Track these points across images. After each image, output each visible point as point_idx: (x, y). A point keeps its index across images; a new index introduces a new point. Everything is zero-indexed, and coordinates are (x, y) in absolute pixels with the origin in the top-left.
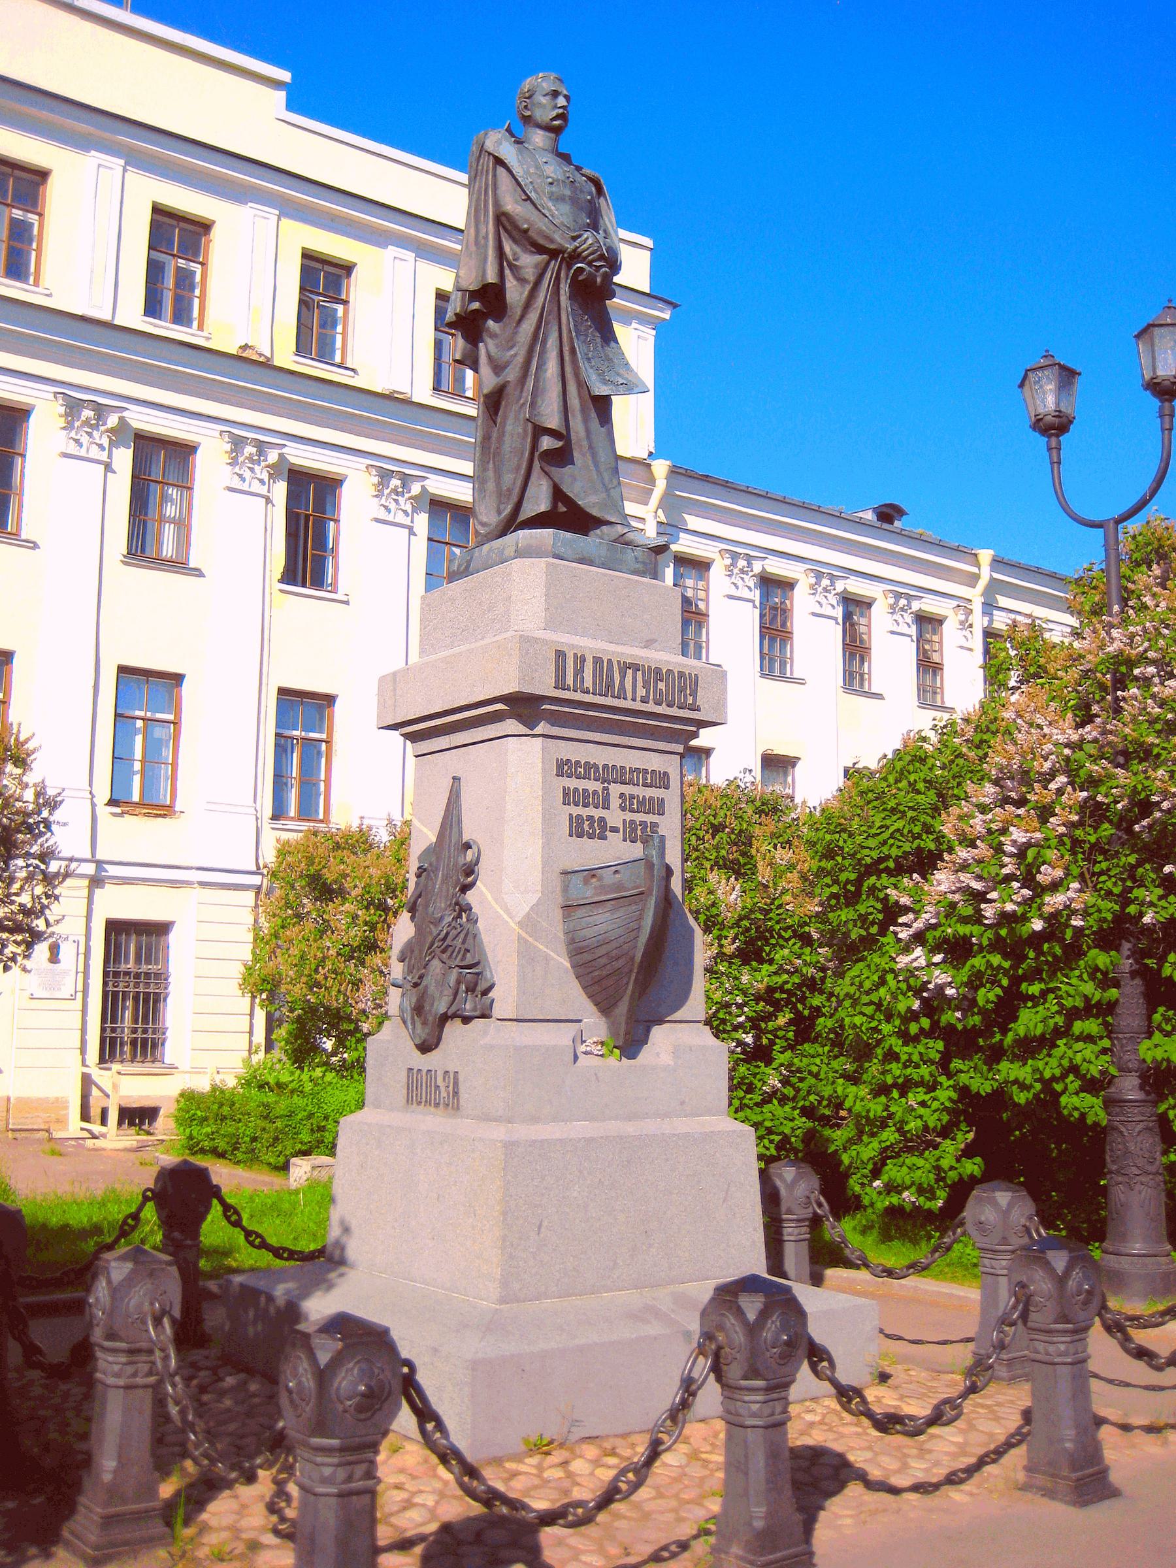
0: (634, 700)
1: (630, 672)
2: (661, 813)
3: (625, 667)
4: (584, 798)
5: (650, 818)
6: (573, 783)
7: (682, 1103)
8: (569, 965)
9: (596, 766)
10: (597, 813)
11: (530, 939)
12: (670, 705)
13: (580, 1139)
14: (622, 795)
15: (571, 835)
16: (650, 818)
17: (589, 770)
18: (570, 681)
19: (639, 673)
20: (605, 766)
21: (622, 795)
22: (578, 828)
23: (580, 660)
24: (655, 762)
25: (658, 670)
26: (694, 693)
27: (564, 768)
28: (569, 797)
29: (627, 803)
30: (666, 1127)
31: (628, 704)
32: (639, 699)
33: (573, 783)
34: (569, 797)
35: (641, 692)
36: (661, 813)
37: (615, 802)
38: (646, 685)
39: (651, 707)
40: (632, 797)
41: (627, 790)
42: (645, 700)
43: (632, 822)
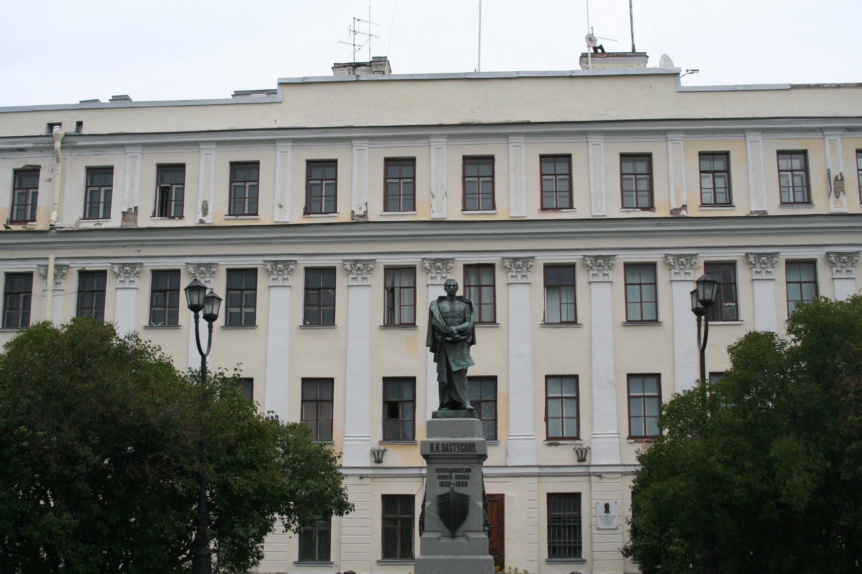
3: (451, 444)
4: (445, 477)
6: (441, 474)
10: (448, 481)
17: (446, 470)
22: (442, 485)
24: (466, 467)
25: (462, 444)
27: (438, 470)
28: (439, 477)
30: (460, 557)
33: (441, 474)
34: (439, 477)
37: (454, 477)
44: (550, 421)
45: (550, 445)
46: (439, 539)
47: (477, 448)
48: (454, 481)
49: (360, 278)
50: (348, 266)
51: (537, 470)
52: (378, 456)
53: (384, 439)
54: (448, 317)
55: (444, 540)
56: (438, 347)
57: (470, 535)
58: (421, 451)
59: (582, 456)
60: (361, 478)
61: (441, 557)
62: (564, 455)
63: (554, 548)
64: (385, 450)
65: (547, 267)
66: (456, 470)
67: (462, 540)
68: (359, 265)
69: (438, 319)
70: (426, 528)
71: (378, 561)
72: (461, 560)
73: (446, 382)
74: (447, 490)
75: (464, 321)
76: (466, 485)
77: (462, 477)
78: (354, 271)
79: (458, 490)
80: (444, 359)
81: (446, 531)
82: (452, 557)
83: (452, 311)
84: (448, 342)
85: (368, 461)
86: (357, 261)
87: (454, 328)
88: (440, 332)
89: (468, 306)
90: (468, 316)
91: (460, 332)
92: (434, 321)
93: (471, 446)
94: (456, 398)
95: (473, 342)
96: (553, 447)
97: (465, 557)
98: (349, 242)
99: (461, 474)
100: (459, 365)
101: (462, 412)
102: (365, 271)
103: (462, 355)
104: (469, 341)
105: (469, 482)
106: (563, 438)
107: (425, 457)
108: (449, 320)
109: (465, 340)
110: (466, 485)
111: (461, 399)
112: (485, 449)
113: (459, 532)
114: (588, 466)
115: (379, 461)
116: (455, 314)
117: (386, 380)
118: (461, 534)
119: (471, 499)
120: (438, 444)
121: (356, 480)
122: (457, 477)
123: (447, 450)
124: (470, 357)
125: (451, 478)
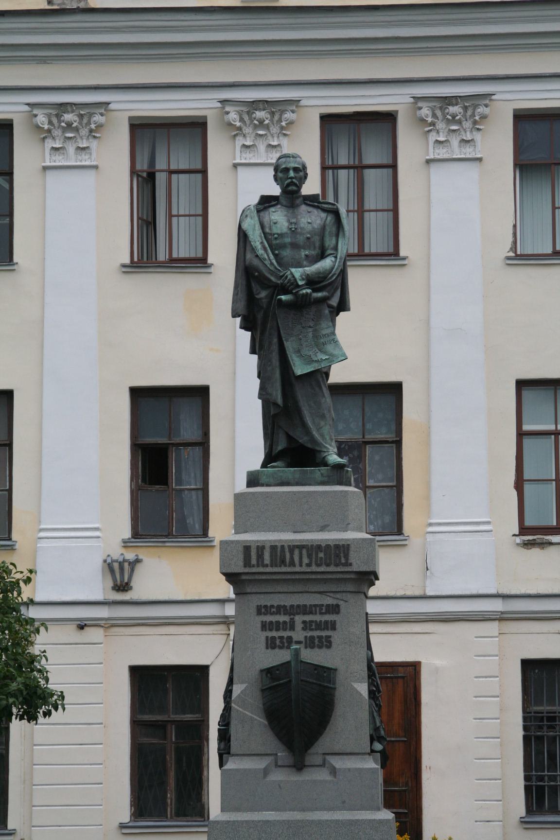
0: (301, 565)
1: (297, 552)
2: (334, 628)
3: (292, 548)
4: (277, 626)
5: (324, 633)
6: (269, 618)
7: (344, 802)
8: (266, 723)
9: (285, 606)
10: (285, 634)
12: (328, 565)
13: (259, 821)
14: (304, 622)
15: (267, 648)
16: (324, 633)
17: (280, 609)
18: (254, 561)
19: (304, 552)
20: (292, 606)
21: (304, 622)
24: (328, 601)
25: (319, 547)
26: (347, 556)
27: (261, 610)
28: (264, 626)
31: (297, 569)
32: (304, 564)
33: (269, 618)
34: (264, 626)
35: (306, 560)
36: (334, 628)
37: (299, 626)
38: (309, 556)
39: (314, 568)
40: (311, 622)
41: (308, 618)
42: (309, 565)
43: (312, 638)
44: (527, 487)
45: (527, 545)
46: (266, 772)
47: (353, 557)
48: (299, 634)
49: (71, 149)
50: (42, 119)
51: (497, 606)
52: (120, 575)
53: (136, 534)
54: (283, 246)
55: (278, 776)
56: (260, 316)
57: (338, 763)
58: (222, 565)
60: (81, 627)
61: (270, 816)
63: (540, 790)
64: (138, 561)
65: (522, 118)
66: (304, 610)
67: (322, 775)
68: (68, 117)
69: (261, 252)
70: (234, 747)
71: (122, 826)
72: (320, 823)
73: (280, 401)
74: (282, 656)
75: (322, 256)
76: (329, 645)
77: (319, 626)
78: (57, 133)
79: (311, 656)
80: (275, 347)
81: (283, 754)
82: (297, 816)
83: (294, 232)
84: (284, 305)
85: (96, 588)
86: (63, 107)
87: (297, 272)
88: (264, 282)
89: (330, 218)
90: (330, 242)
91: (313, 282)
92: (249, 256)
93: (339, 552)
94: (303, 440)
95: (343, 306)
96: (535, 551)
97: (326, 816)
98: (44, 60)
99: (317, 618)
100: (310, 361)
101: (318, 472)
102: (84, 132)
103: (316, 337)
104: (334, 302)
105: (336, 637)
107: (231, 577)
108: (287, 253)
109: (324, 300)
110: (329, 645)
111: (313, 440)
112: (372, 558)
113: (313, 756)
115: (123, 587)
116: (301, 239)
117: (137, 393)
118: (318, 760)
119: (340, 677)
120: (261, 549)
121: (69, 633)
122: (307, 626)
123: (283, 562)
124: (335, 342)
125: (292, 628)
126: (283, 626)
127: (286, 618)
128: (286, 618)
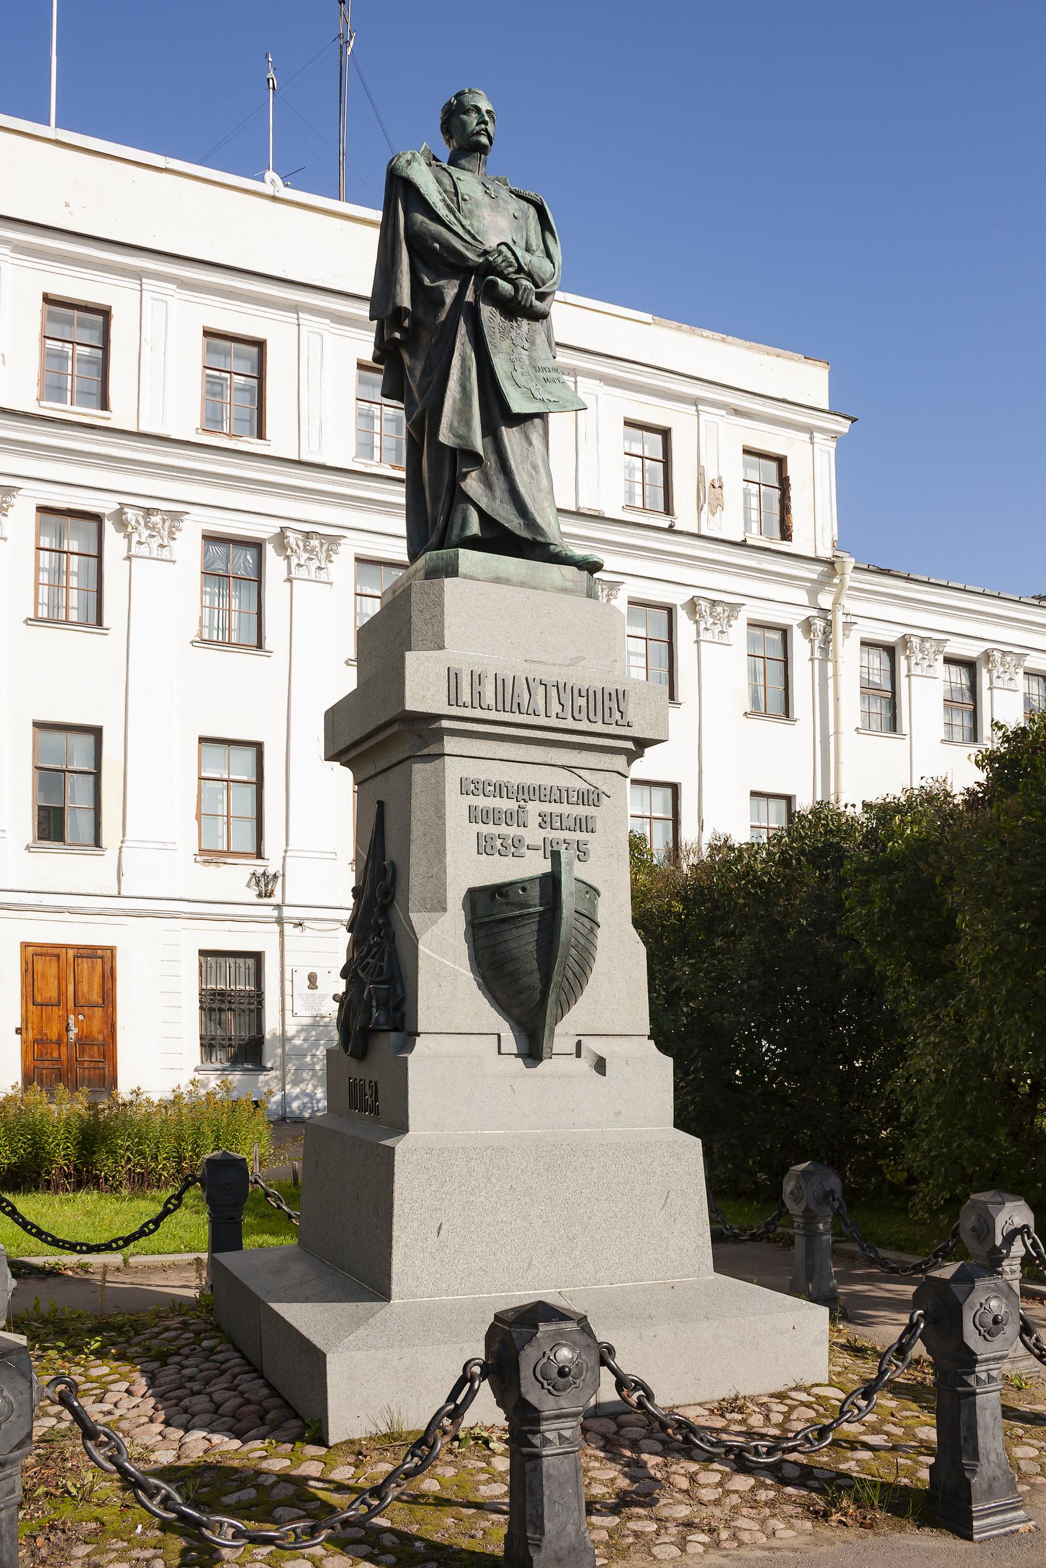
6: (482, 802)
11: (435, 956)
17: (500, 790)
22: (485, 846)
23: (477, 679)
28: (475, 815)
29: (546, 821)
33: (482, 802)
59: (265, 885)
62: (233, 880)
93: (611, 701)
96: (212, 868)
106: (228, 853)
114: (278, 907)
126: (509, 818)
127: (511, 805)
128: (511, 805)
